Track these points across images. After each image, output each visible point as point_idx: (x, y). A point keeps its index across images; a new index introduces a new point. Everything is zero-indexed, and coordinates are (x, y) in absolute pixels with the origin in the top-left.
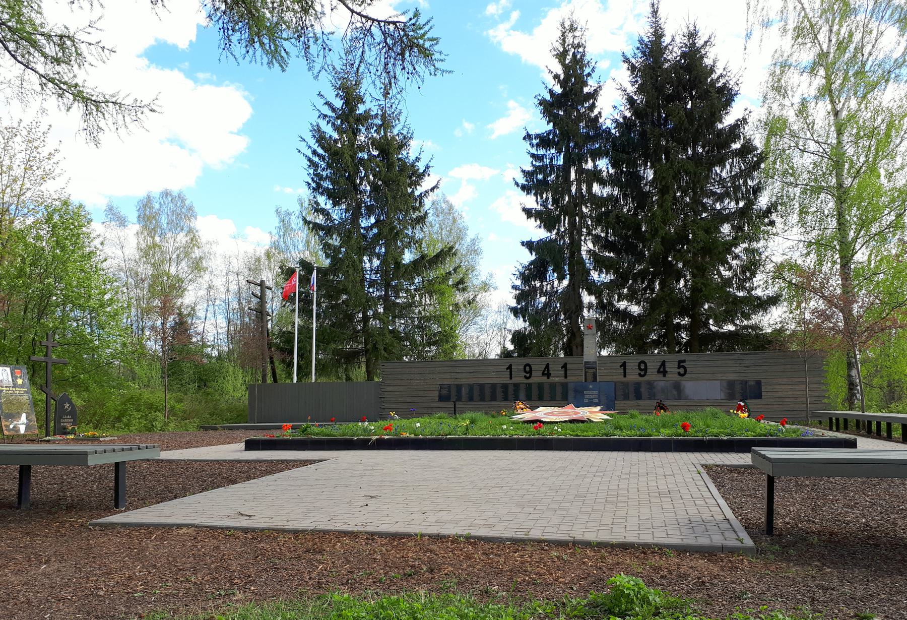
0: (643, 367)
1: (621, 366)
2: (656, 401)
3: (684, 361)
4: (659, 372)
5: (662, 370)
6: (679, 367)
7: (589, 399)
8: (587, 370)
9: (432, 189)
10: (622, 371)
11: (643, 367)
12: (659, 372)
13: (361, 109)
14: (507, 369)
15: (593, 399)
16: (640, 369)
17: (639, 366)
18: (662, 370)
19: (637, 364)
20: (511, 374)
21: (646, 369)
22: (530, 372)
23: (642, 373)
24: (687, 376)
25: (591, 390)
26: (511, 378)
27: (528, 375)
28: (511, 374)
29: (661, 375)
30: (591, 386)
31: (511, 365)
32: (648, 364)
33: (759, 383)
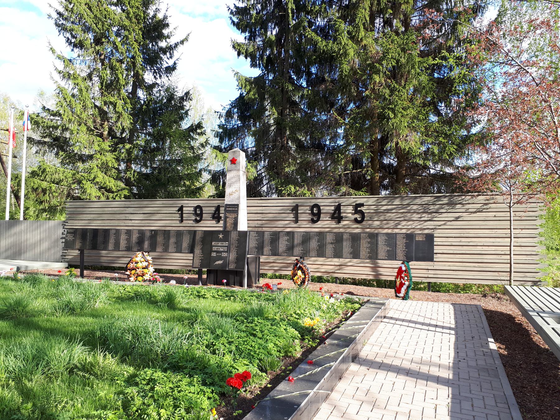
2: (295, 258)
3: (362, 205)
6: (356, 211)
7: (217, 252)
8: (228, 215)
9: (182, 42)
14: (179, 211)
15: (221, 252)
16: (313, 213)
17: (312, 210)
20: (182, 217)
22: (201, 215)
24: (364, 223)
25: (221, 240)
27: (198, 219)
28: (182, 217)
30: (221, 236)
33: (430, 238)
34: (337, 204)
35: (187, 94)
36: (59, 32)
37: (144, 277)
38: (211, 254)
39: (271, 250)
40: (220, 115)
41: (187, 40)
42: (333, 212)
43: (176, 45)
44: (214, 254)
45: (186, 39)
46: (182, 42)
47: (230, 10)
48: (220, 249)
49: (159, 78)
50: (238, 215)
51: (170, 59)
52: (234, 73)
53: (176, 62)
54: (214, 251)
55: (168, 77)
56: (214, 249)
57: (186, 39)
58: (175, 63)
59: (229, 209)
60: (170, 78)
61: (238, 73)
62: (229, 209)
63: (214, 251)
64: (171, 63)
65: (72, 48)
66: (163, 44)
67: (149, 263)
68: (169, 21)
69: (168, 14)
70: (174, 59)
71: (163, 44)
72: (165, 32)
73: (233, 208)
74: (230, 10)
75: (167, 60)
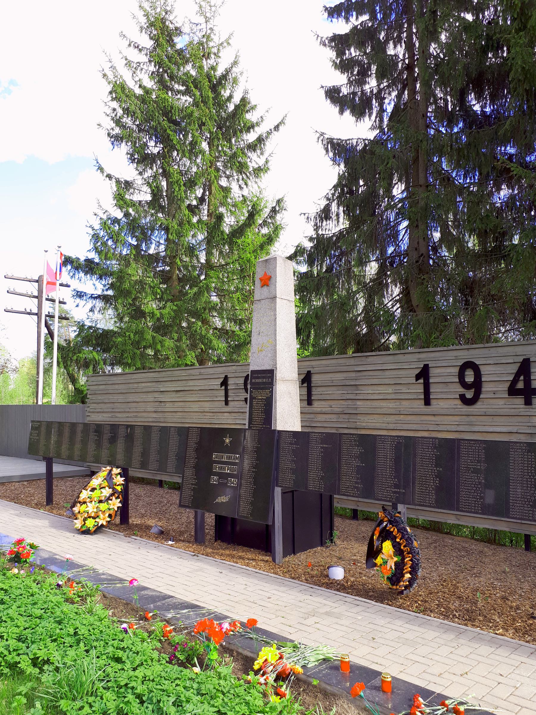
0: (470, 377)
1: (418, 377)
4: (513, 391)
5: (520, 385)
8: (256, 393)
9: (277, 128)
10: (420, 389)
11: (470, 377)
12: (513, 391)
13: (180, 42)
16: (462, 382)
18: (520, 385)
19: (457, 370)
20: (226, 396)
21: (477, 385)
23: (469, 395)
26: (227, 403)
28: (226, 396)
29: (519, 401)
31: (226, 379)
32: (484, 370)
34: (521, 359)
35: (279, 202)
36: (113, 144)
37: (97, 520)
38: (209, 479)
39: (322, 478)
40: (308, 218)
41: (284, 123)
42: (511, 378)
43: (269, 133)
44: (214, 480)
45: (282, 122)
46: (277, 128)
47: (319, 38)
48: (224, 469)
49: (245, 187)
50: (272, 392)
51: (261, 156)
52: (318, 135)
53: (269, 158)
54: (216, 474)
55: (256, 182)
56: (217, 468)
57: (282, 122)
58: (267, 162)
59: (257, 381)
60: (259, 183)
61: (322, 134)
62: (257, 381)
63: (216, 474)
64: (261, 162)
65: (135, 165)
66: (251, 137)
67: (114, 489)
68: (253, 100)
69: (249, 87)
70: (266, 155)
71: (251, 137)
72: (251, 117)
73: (264, 378)
74: (319, 38)
75: (258, 160)
